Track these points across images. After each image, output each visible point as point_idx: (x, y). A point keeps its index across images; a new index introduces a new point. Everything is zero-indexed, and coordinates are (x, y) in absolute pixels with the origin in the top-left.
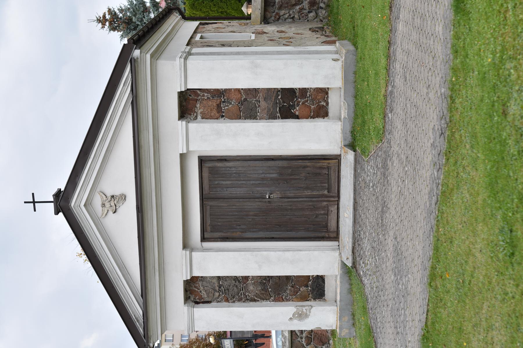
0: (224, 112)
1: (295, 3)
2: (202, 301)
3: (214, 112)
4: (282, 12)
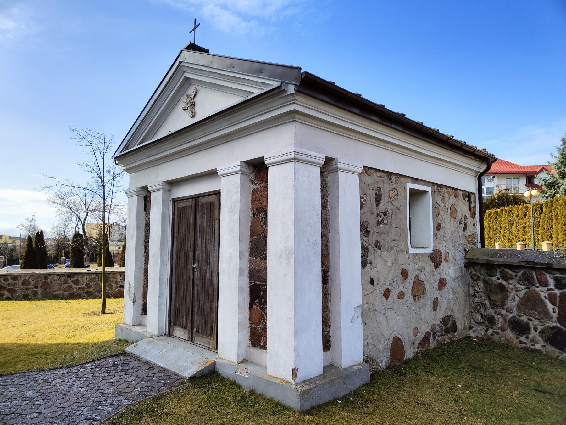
0: (257, 216)
1: (492, 299)
2: (147, 203)
3: (258, 204)
4: (481, 284)
